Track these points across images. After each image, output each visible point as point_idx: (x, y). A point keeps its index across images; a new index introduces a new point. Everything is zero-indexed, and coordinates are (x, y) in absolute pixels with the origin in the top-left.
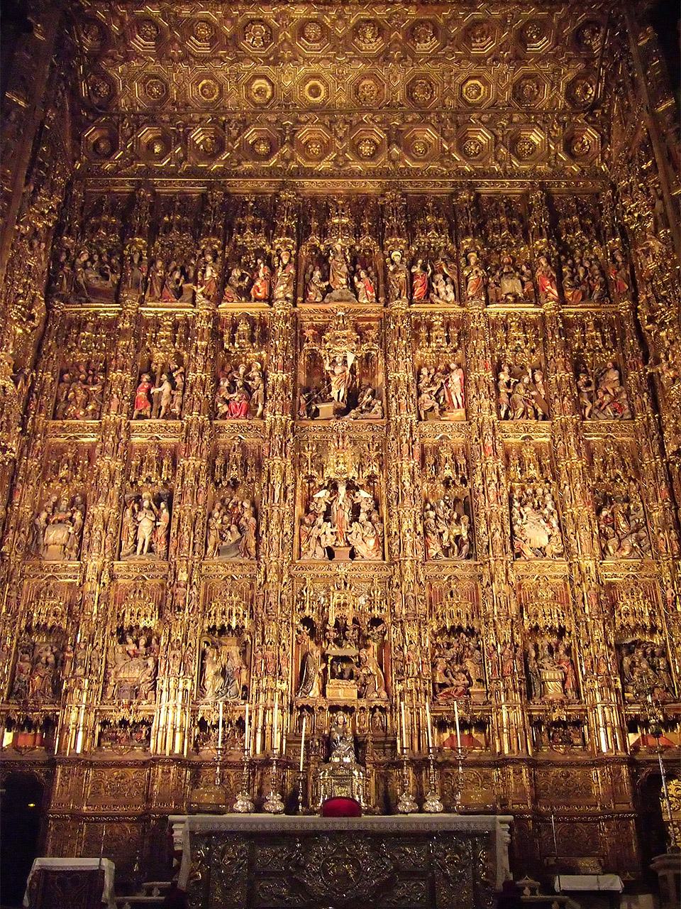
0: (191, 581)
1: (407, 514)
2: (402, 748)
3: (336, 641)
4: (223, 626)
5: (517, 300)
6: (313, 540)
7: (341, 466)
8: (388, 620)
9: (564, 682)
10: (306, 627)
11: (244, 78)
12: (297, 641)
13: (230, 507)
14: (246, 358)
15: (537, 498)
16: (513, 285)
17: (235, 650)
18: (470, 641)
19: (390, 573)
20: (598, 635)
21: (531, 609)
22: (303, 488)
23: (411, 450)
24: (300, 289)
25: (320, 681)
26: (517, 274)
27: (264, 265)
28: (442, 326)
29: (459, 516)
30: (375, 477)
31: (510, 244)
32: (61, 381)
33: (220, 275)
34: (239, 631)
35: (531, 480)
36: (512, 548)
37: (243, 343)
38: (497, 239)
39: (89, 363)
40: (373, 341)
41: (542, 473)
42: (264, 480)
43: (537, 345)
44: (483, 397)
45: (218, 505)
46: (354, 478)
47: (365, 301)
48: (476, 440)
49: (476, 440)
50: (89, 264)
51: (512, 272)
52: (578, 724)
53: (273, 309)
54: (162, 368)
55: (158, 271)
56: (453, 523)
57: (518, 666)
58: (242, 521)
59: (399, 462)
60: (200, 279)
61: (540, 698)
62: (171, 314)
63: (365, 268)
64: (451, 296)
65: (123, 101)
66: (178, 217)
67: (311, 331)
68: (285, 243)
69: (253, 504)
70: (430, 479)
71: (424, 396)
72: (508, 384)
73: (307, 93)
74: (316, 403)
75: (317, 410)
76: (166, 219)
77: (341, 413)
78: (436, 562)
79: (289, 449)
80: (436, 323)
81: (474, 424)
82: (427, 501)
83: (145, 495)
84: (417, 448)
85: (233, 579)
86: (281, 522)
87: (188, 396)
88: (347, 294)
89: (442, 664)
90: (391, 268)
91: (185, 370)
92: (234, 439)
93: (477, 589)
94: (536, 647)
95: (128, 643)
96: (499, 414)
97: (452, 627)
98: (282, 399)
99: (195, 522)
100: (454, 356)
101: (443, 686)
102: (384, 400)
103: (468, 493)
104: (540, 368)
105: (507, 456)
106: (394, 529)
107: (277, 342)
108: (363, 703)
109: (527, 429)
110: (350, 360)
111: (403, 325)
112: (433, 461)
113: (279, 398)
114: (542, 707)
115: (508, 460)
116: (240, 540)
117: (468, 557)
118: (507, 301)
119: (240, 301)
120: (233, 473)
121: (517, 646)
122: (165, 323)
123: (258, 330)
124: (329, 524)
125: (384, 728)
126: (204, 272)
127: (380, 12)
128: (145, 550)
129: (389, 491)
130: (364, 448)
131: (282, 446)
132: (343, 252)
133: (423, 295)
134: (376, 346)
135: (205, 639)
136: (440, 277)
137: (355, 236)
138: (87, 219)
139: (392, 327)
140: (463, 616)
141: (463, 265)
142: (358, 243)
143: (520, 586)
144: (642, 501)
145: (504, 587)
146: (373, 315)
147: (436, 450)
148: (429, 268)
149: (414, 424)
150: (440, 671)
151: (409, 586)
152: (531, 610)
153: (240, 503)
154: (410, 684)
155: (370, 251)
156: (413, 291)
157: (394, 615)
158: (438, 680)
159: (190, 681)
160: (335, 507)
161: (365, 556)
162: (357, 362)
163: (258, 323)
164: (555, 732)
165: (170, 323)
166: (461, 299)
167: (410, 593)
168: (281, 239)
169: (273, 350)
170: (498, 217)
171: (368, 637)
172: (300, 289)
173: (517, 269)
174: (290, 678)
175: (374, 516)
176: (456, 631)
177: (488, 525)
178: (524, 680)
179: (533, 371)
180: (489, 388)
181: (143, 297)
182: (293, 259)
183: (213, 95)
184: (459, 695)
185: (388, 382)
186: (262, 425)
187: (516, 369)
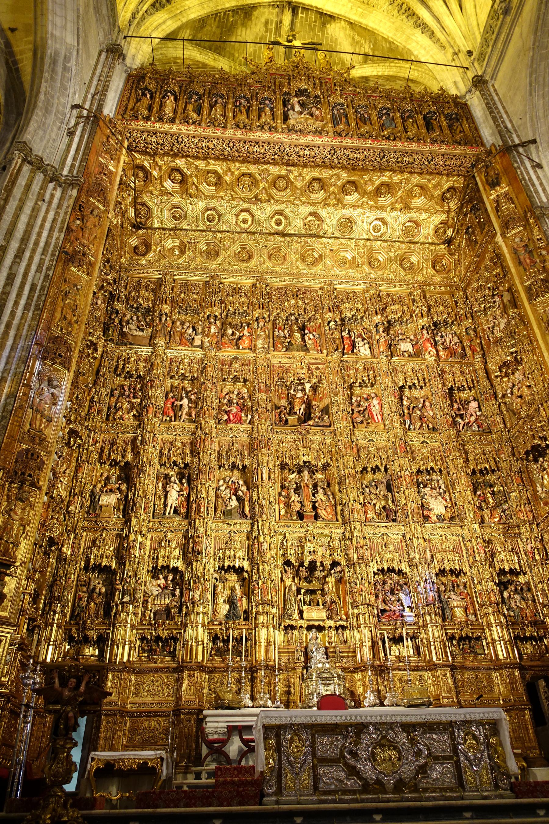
3: (306, 579)
8: (343, 563)
9: (466, 609)
11: (234, 211)
19: (342, 531)
20: (487, 575)
21: (439, 556)
26: (408, 340)
32: (112, 395)
34: (240, 571)
39: (131, 385)
45: (221, 482)
50: (131, 321)
52: (478, 638)
58: (240, 493)
65: (155, 221)
73: (273, 224)
95: (159, 579)
101: (383, 611)
127: (326, 174)
138: (130, 293)
144: (502, 486)
150: (381, 600)
154: (361, 609)
157: (348, 559)
164: (463, 645)
176: (391, 570)
179: (424, 401)
183: (214, 221)
184: (397, 617)
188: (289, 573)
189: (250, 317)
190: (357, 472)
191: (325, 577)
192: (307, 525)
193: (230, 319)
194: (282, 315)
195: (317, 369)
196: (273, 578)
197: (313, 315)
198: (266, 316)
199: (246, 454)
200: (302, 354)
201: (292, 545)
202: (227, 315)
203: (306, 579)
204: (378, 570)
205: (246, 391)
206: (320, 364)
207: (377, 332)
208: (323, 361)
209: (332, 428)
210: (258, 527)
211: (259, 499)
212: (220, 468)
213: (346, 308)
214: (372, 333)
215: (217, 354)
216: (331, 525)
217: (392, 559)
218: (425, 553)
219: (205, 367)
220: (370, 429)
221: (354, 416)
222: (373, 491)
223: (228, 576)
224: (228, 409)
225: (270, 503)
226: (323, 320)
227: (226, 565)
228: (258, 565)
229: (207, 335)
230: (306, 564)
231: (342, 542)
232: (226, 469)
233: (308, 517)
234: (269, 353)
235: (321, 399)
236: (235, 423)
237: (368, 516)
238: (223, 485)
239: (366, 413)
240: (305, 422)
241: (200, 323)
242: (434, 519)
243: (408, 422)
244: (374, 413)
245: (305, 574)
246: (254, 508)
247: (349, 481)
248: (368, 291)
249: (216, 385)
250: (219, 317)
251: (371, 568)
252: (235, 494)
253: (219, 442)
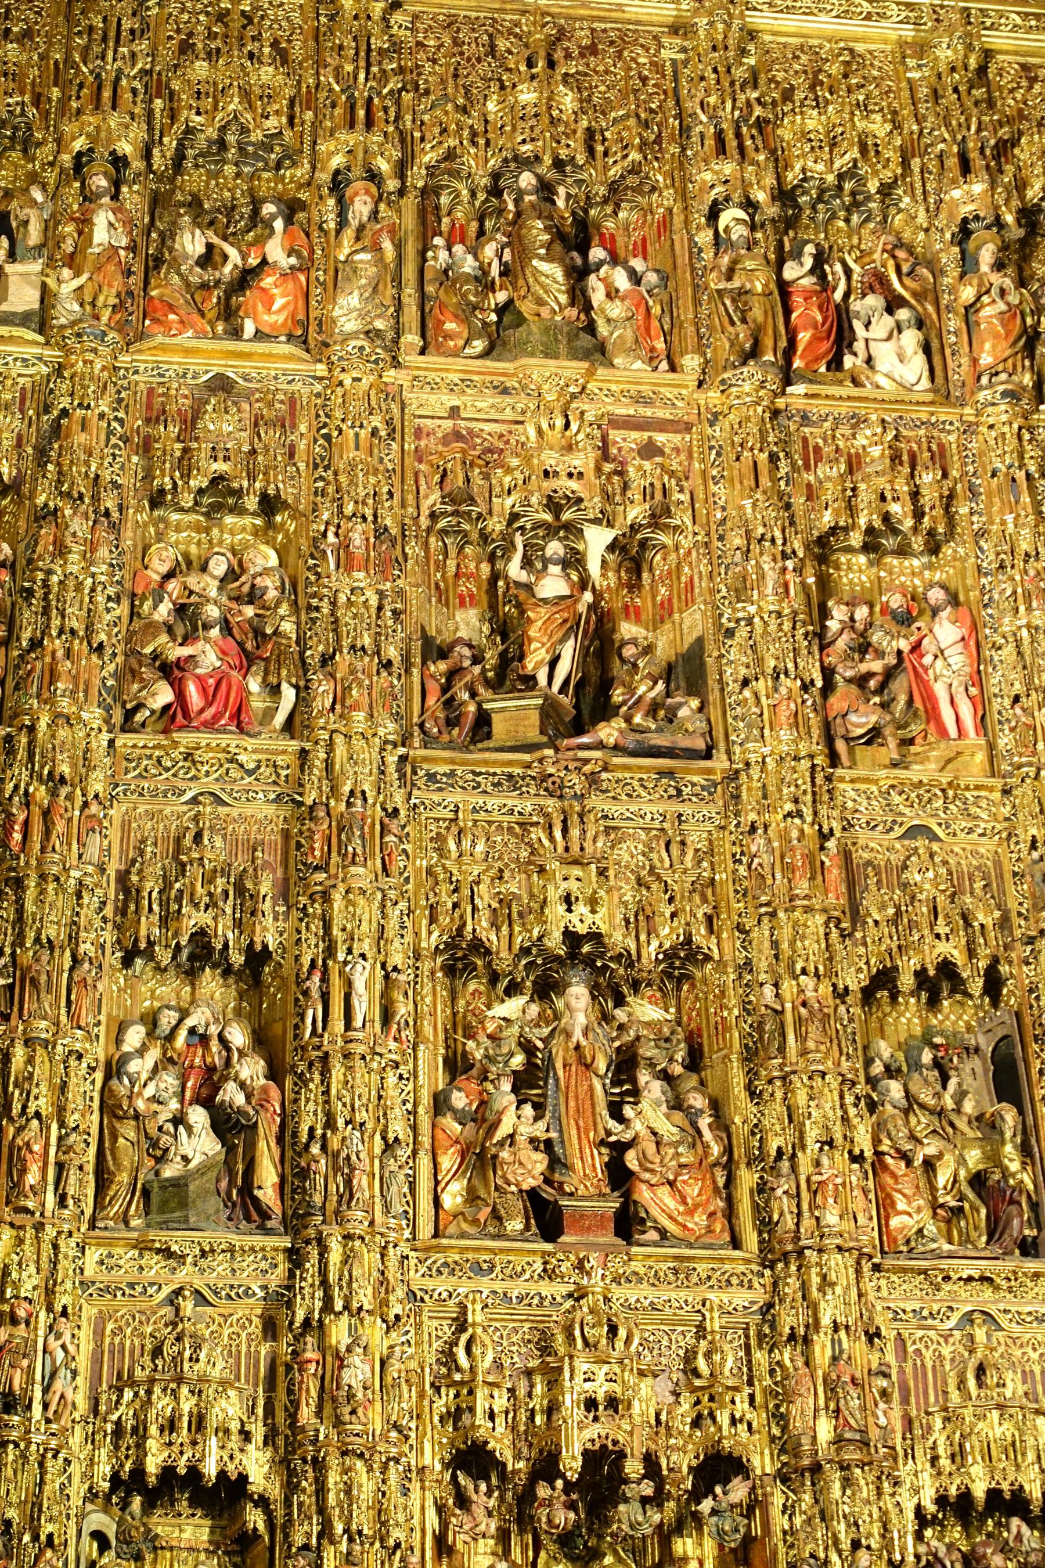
19: (759, 1296)
45: (135, 1036)
58: (232, 1094)
135: (99, 1520)
188: (479, 1512)
189: (302, 171)
190: (841, 994)
191: (665, 1535)
192: (580, 1266)
193: (193, 179)
194: (470, 160)
195: (649, 450)
196: (397, 1534)
197: (634, 170)
198: (383, 166)
199: (265, 888)
200: (572, 369)
201: (497, 1364)
202: (179, 157)
203: (566, 1540)
204: (941, 1501)
205: (273, 561)
206: (662, 426)
207: (967, 264)
208: (681, 411)
209: (720, 763)
210: (323, 1272)
211: (330, 1123)
212: (127, 962)
213: (805, 136)
214: (937, 272)
215: (125, 359)
216: (702, 1268)
217: (1013, 1449)
219: (56, 429)
220: (916, 773)
221: (837, 703)
222: (926, 1097)
223: (162, 1525)
225: (390, 1146)
226: (683, 195)
227: (152, 1466)
228: (319, 1465)
229: (72, 261)
230: (572, 1463)
231: (760, 1356)
232: (160, 970)
233: (584, 1222)
234: (396, 363)
235: (665, 612)
236: (210, 725)
237: (895, 1222)
238: (141, 1052)
239: (899, 687)
240: (580, 731)
241: (38, 195)
244: (940, 691)
245: (563, 1517)
246: (304, 1174)
247: (801, 1038)
248: (922, 49)
249: (115, 528)
250: (137, 164)
251: (904, 1491)
252: (207, 1101)
253: (125, 826)
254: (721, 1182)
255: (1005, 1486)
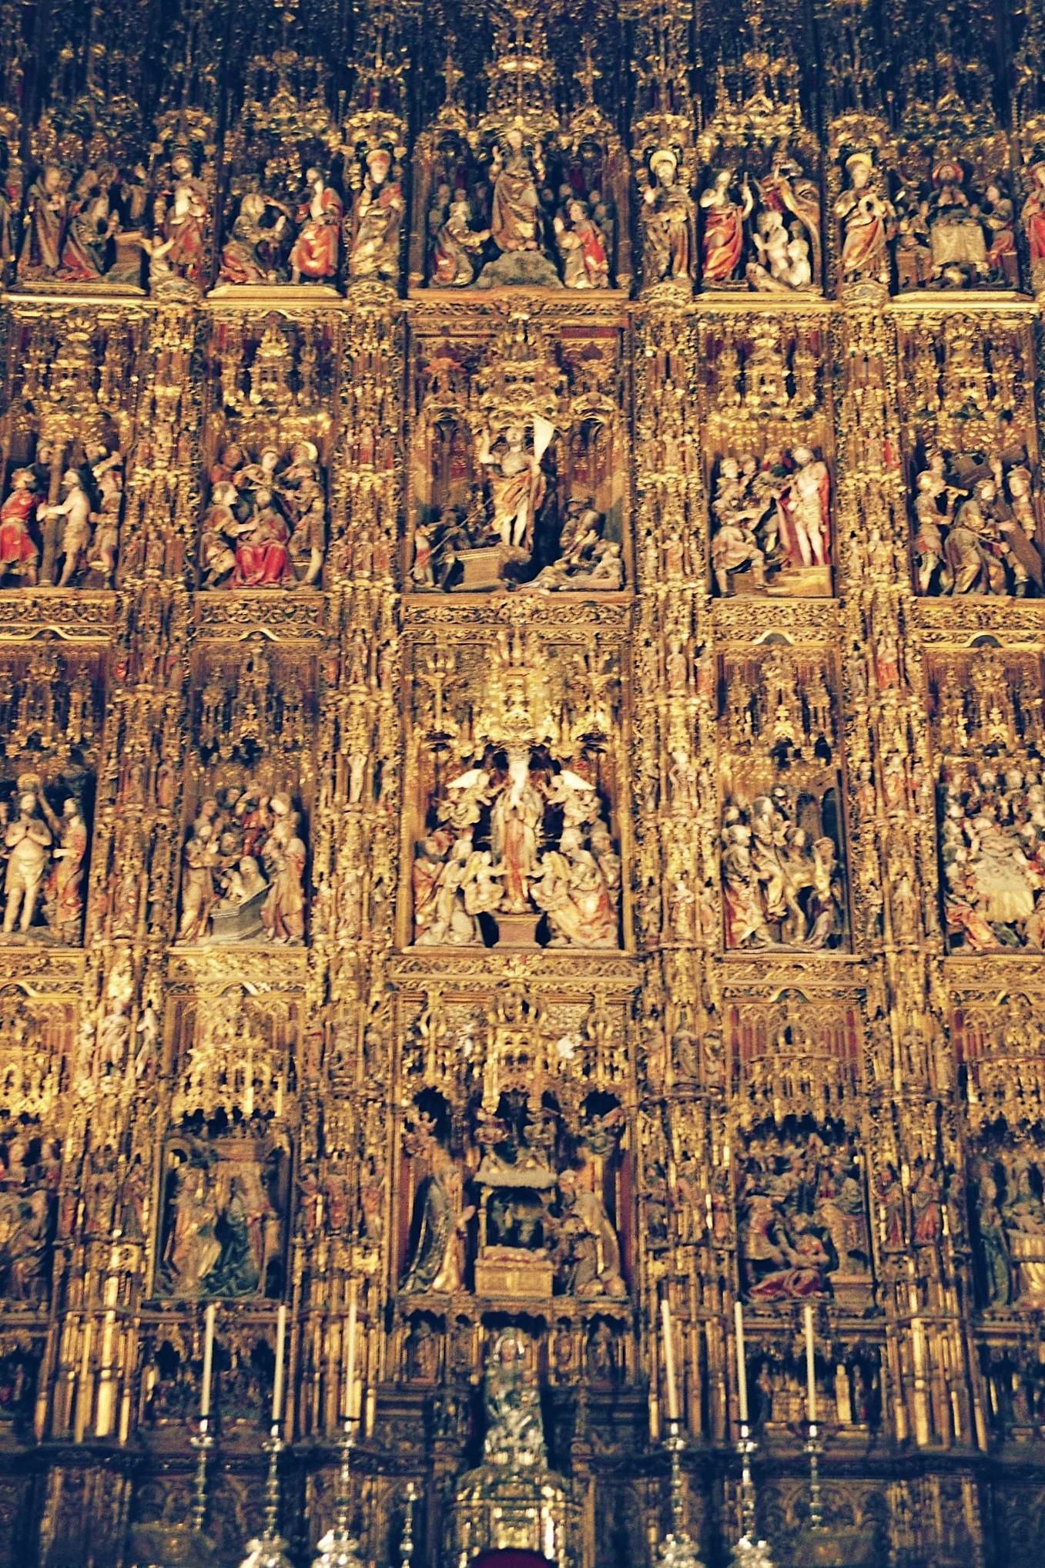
0: (140, 998)
1: (680, 833)
2: (665, 1421)
4: (220, 1111)
5: (972, 281)
6: (444, 897)
7: (518, 710)
8: (630, 1098)
10: (426, 1115)
12: (404, 1149)
13: (241, 808)
14: (280, 428)
15: (1008, 795)
16: (962, 243)
17: (250, 1172)
18: (832, 1154)
19: (635, 980)
22: (421, 762)
23: (693, 671)
24: (417, 250)
25: (461, 1251)
26: (975, 210)
27: (327, 184)
28: (777, 351)
29: (809, 839)
30: (602, 738)
31: (957, 128)
33: (210, 211)
35: (993, 750)
36: (942, 920)
37: (271, 392)
38: (926, 114)
40: (600, 388)
41: (1020, 731)
42: (326, 744)
43: (1020, 400)
44: (876, 536)
45: (209, 808)
46: (548, 739)
47: (582, 284)
48: (856, 648)
49: (856, 648)
51: (960, 206)
53: (346, 303)
54: (67, 453)
55: (49, 198)
56: (795, 856)
57: (950, 1221)
59: (661, 701)
60: (159, 220)
61: (1009, 1303)
62: (87, 312)
63: (582, 194)
64: (802, 273)
66: (99, 50)
67: (446, 361)
68: (379, 128)
69: (296, 804)
70: (739, 744)
71: (728, 533)
72: (941, 501)
74: (457, 548)
75: (459, 566)
76: (66, 53)
77: (519, 573)
78: (752, 954)
79: (386, 665)
80: (760, 342)
81: (852, 605)
82: (729, 802)
83: (27, 779)
84: (706, 665)
85: (245, 991)
86: (366, 853)
87: (134, 528)
88: (537, 264)
89: (761, 1209)
90: (650, 196)
91: (125, 460)
92: (249, 639)
93: (851, 1023)
94: (999, 1174)
96: (914, 579)
97: (789, 1119)
98: (371, 539)
99: (152, 851)
100: (804, 428)
102: (628, 542)
103: (832, 781)
104: (1024, 462)
105: (934, 688)
106: (647, 873)
107: (359, 391)
108: (566, 1307)
109: (984, 620)
110: (542, 442)
111: (681, 349)
112: (745, 701)
113: (365, 535)
114: (1013, 1326)
115: (937, 700)
116: (265, 894)
117: (832, 942)
118: (944, 284)
119: (262, 281)
120: (248, 727)
121: (951, 1169)
122: (70, 337)
123: (309, 358)
124: (486, 857)
125: (617, 1373)
126: (171, 201)
128: (25, 920)
129: (636, 774)
130: (575, 666)
131: (369, 656)
132: (528, 152)
133: (727, 269)
134: (609, 403)
136: (774, 219)
137: (559, 110)
139: (649, 354)
140: (816, 1092)
141: (835, 187)
142: (566, 126)
143: (959, 1017)
145: (918, 1021)
146: (601, 321)
147: (754, 672)
148: (747, 194)
149: (700, 604)
151: (683, 1015)
152: (987, 1081)
153: (264, 801)
154: (682, 1261)
155: (596, 149)
156: (703, 258)
157: (644, 1085)
158: (752, 1251)
159: (135, 1251)
160: (500, 814)
161: (577, 939)
162: (559, 443)
163: (309, 339)
165: (84, 337)
166: (827, 279)
167: (684, 1033)
168: (369, 116)
169: (347, 410)
170: (930, 55)
171: (581, 1140)
172: (417, 250)
173: (975, 197)
174: (384, 1242)
175: (599, 836)
176: (797, 1127)
177: (883, 866)
178: (967, 1256)
179: (1006, 469)
180: (892, 512)
181: (14, 265)
182: (398, 170)
184: (806, 1291)
185: (637, 494)
186: (318, 604)
187: (964, 464)
218: (928, 1059)
223: (219, 1146)
224: (236, 530)
237: (735, 927)
242: (984, 935)
243: (930, 564)
254: (614, 900)
255: (799, 1113)
